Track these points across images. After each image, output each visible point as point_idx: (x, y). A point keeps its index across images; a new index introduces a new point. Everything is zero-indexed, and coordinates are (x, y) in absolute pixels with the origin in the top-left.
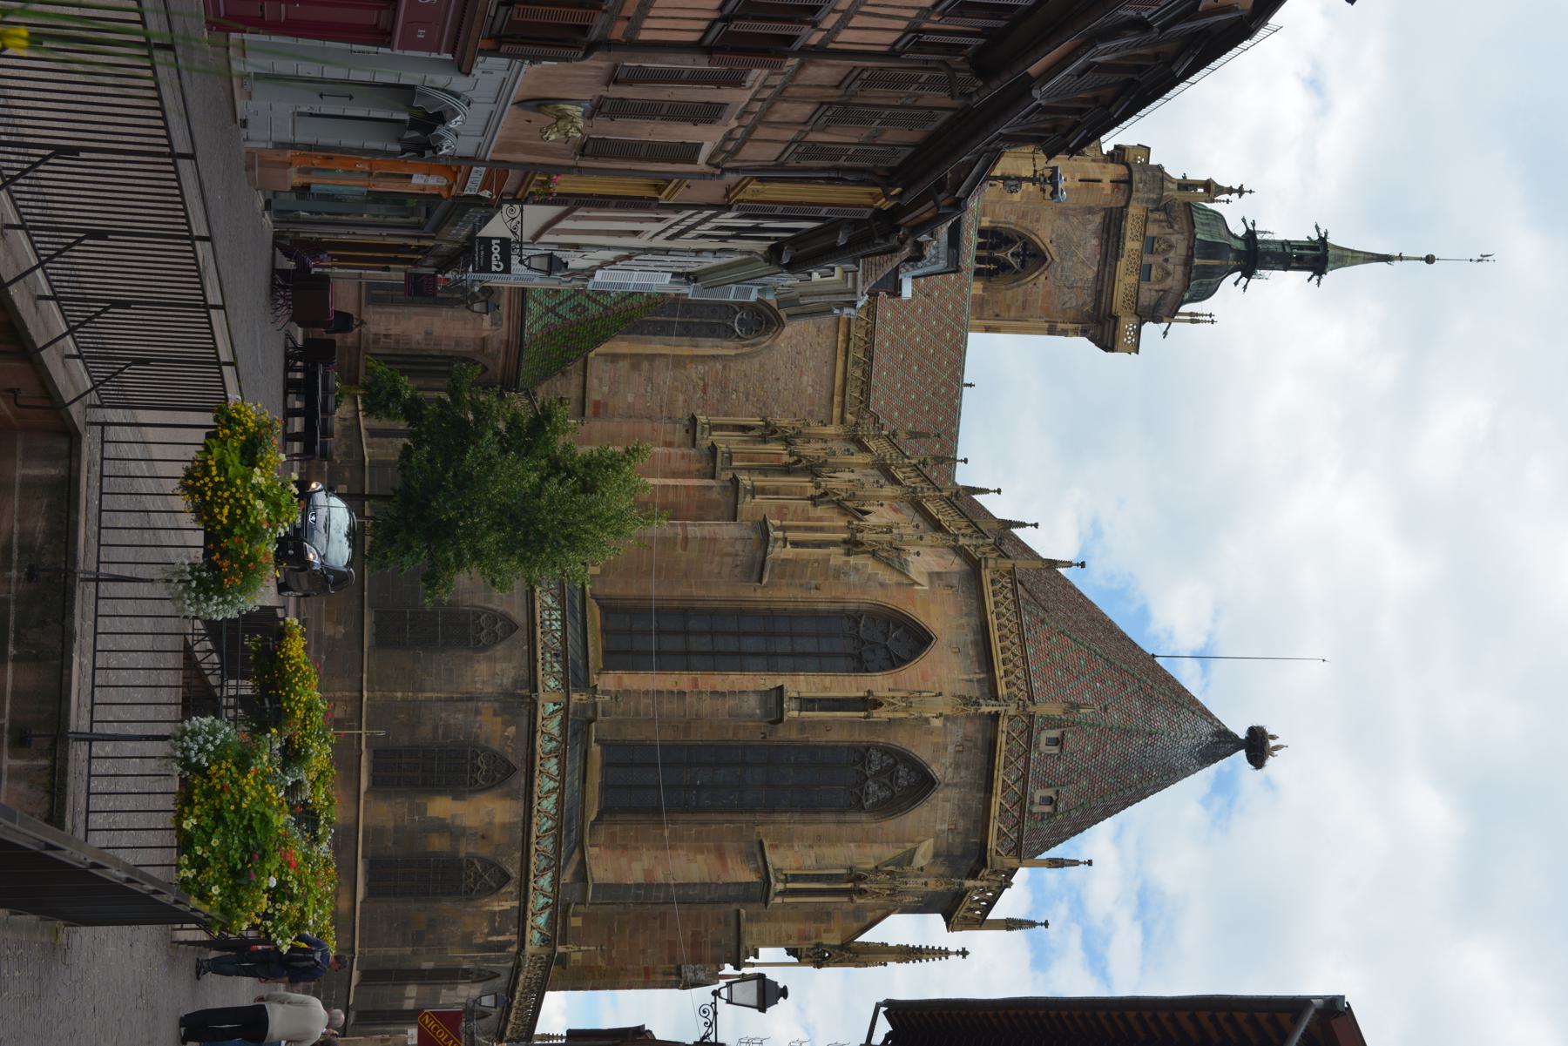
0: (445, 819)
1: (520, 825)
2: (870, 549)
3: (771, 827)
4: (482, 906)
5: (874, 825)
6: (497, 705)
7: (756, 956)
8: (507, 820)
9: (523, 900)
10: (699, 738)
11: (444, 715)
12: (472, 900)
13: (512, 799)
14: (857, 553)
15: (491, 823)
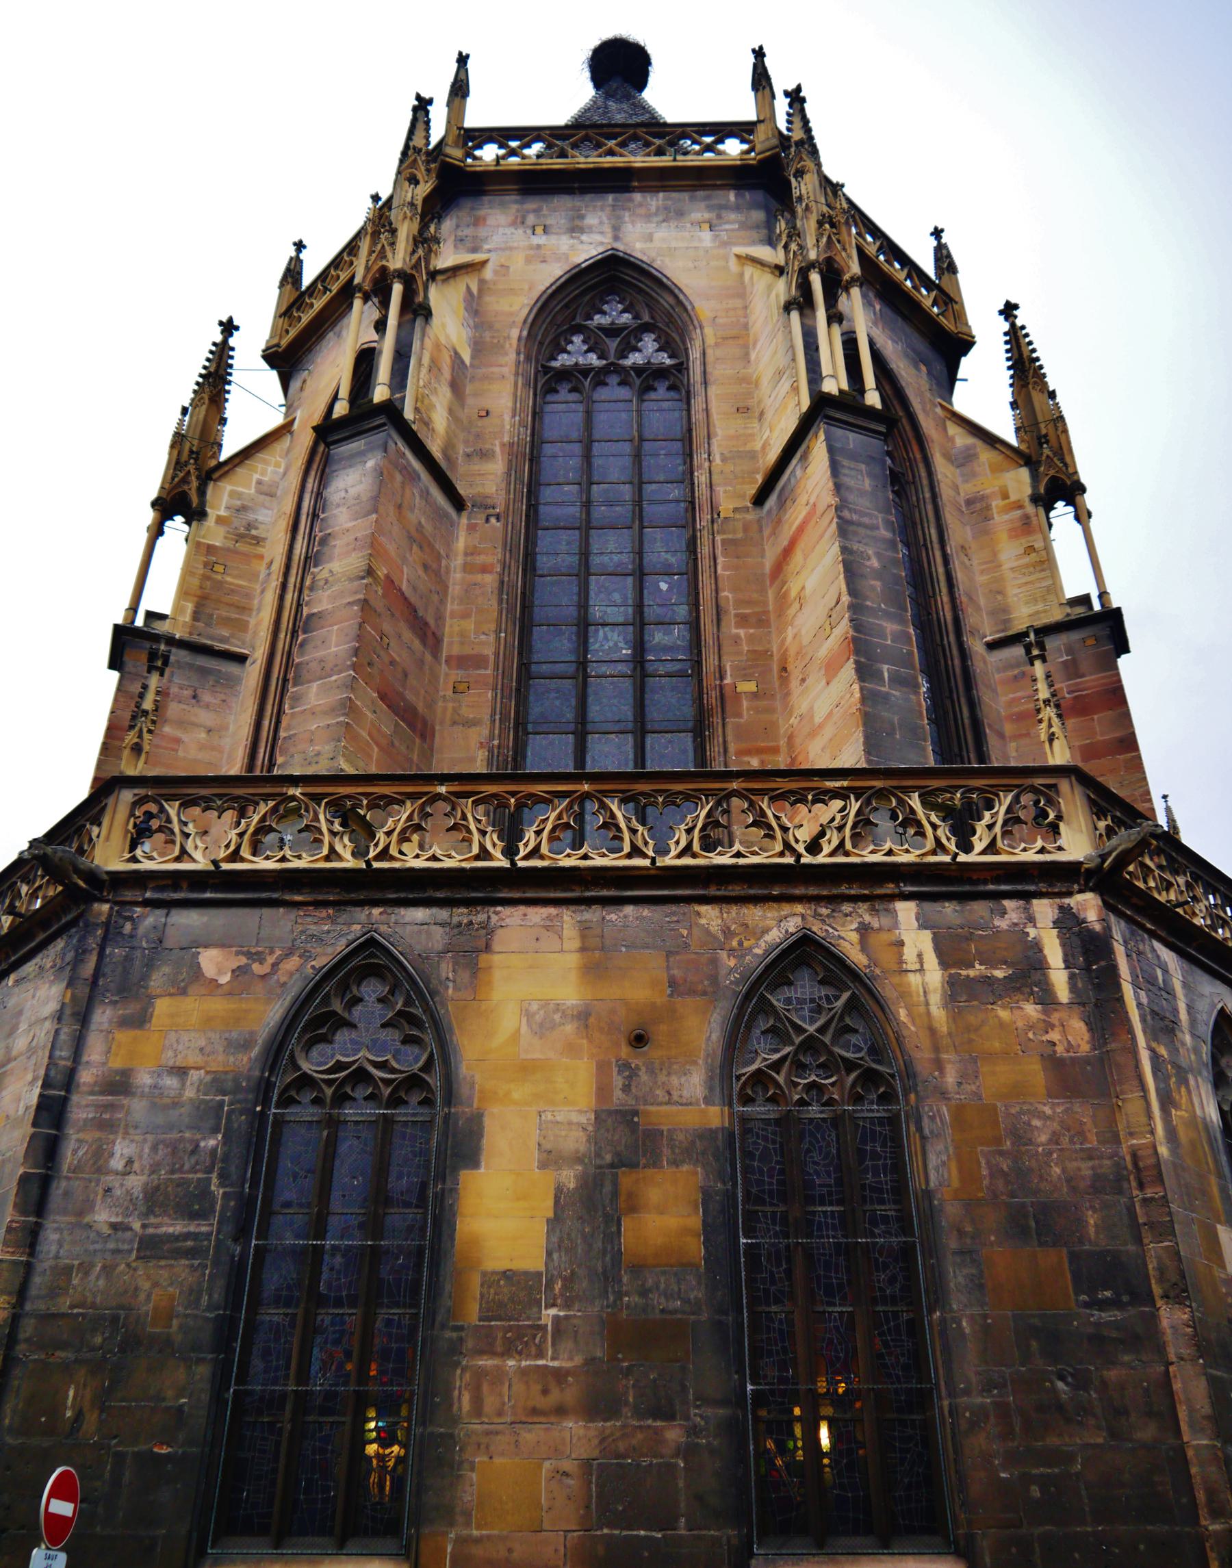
0: (559, 1191)
1: (592, 915)
2: (195, 483)
3: (720, 490)
4: (932, 1031)
5: (708, 331)
6: (102, 1017)
7: (1085, 600)
8: (573, 960)
9: (890, 888)
10: (492, 638)
11: (102, 1216)
12: (909, 1073)
13: (488, 948)
14: (203, 503)
15: (583, 1016)
